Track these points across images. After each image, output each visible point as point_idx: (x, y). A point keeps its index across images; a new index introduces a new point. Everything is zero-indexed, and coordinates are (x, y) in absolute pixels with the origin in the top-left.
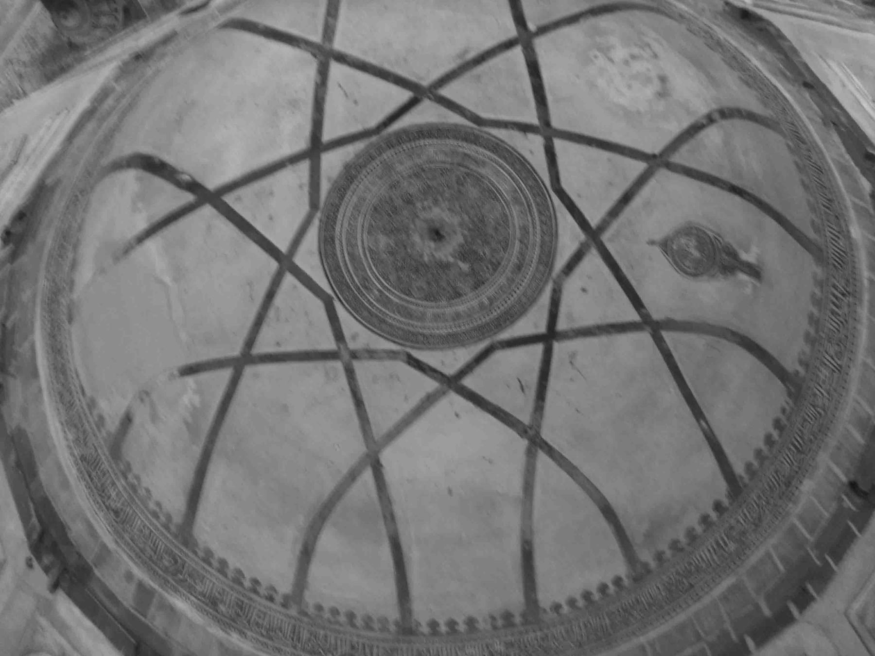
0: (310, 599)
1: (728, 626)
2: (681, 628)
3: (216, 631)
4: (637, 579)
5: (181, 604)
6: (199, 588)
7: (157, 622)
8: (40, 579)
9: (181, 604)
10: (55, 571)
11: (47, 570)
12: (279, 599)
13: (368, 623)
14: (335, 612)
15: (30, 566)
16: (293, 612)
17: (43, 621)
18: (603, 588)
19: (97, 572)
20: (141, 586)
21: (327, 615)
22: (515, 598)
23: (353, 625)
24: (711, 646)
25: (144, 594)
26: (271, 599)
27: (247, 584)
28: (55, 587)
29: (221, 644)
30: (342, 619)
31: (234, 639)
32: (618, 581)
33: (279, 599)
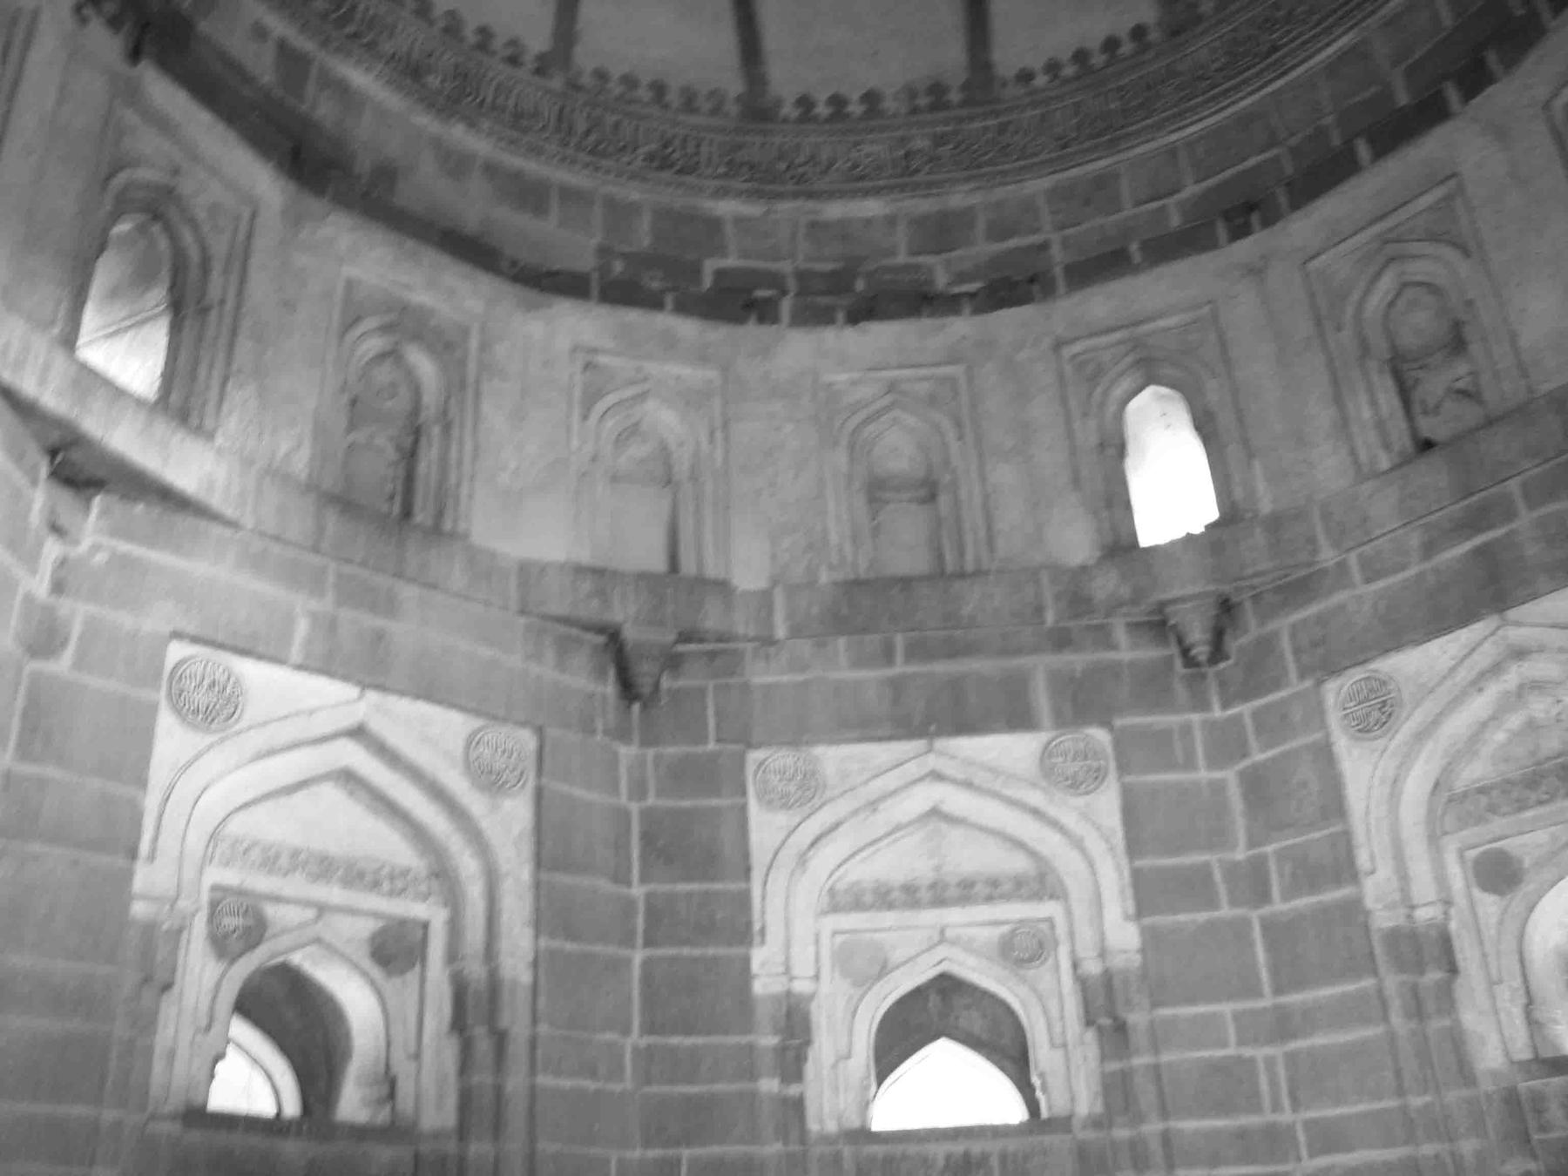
0: (585, 58)
1: (1329, 120)
2: (1245, 121)
3: (425, 121)
4: (1175, 32)
5: (360, 77)
6: (387, 47)
7: (324, 110)
8: (106, 44)
9: (360, 77)
10: (127, 27)
11: (114, 23)
12: (529, 59)
13: (689, 101)
14: (630, 81)
15: (84, 21)
16: (557, 83)
17: (130, 117)
18: (1111, 44)
19: (204, 26)
20: (283, 46)
21: (616, 89)
22: (951, 58)
23: (666, 106)
24: (1295, 152)
25: (292, 62)
26: (514, 61)
27: (471, 37)
28: (135, 55)
29: (437, 143)
30: (644, 93)
31: (458, 133)
32: (1139, 32)
33: (529, 59)
